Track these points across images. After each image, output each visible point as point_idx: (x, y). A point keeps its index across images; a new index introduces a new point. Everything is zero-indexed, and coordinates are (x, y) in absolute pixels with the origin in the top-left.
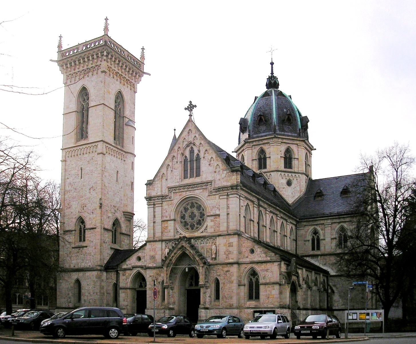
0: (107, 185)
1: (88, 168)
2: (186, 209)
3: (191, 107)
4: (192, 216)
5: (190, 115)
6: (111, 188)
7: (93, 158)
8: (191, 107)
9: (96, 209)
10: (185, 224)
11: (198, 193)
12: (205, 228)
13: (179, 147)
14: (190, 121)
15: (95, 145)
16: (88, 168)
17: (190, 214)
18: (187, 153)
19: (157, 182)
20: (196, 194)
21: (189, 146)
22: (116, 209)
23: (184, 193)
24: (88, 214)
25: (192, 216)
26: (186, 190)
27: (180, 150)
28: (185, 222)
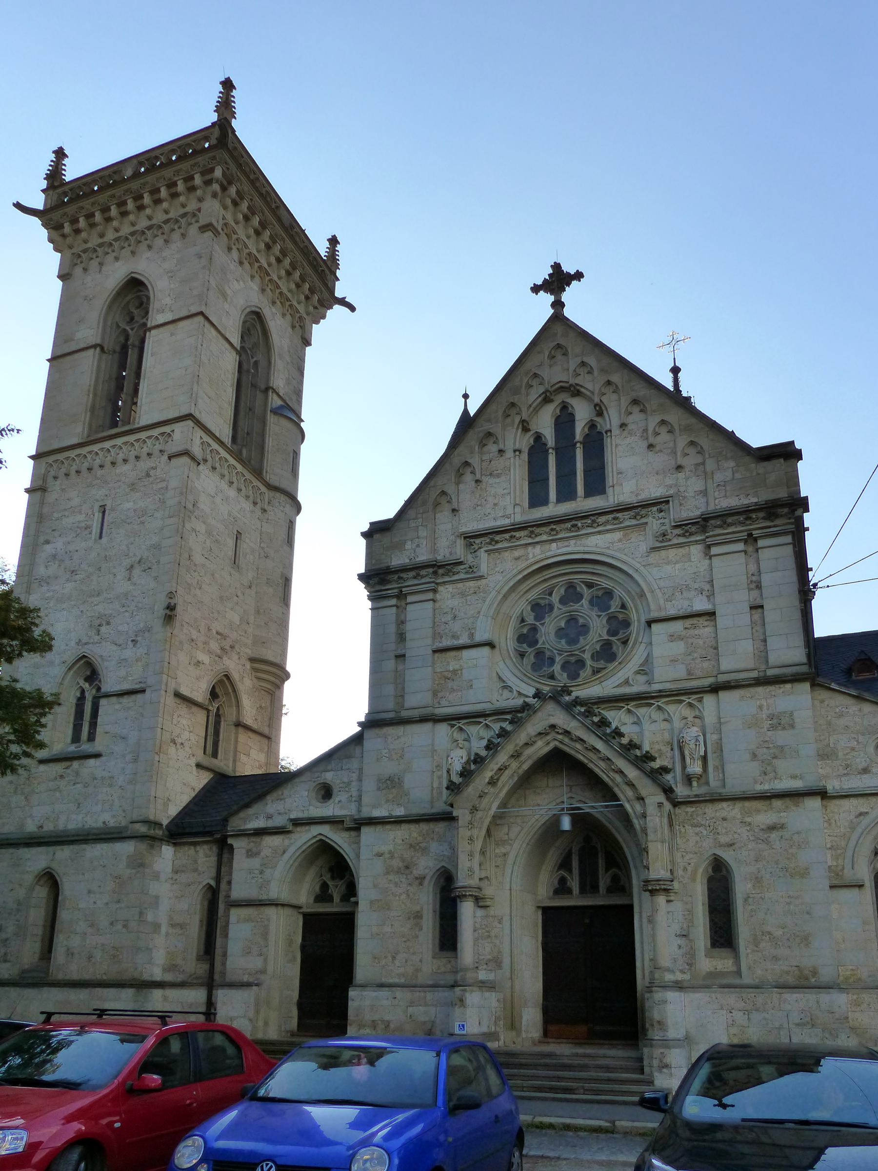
0: (198, 559)
1: (130, 505)
2: (540, 609)
3: (558, 281)
4: (574, 630)
5: (558, 305)
6: (213, 575)
7: (152, 473)
8: (558, 281)
9: (148, 630)
10: (542, 660)
11: (598, 543)
12: (636, 668)
13: (513, 405)
14: (558, 318)
15: (163, 434)
16: (130, 505)
17: (563, 624)
18: (545, 424)
19: (413, 524)
20: (586, 549)
21: (551, 401)
22: (227, 644)
23: (538, 549)
24: (115, 648)
25: (574, 630)
26: (544, 537)
27: (513, 411)
28: (539, 654)
